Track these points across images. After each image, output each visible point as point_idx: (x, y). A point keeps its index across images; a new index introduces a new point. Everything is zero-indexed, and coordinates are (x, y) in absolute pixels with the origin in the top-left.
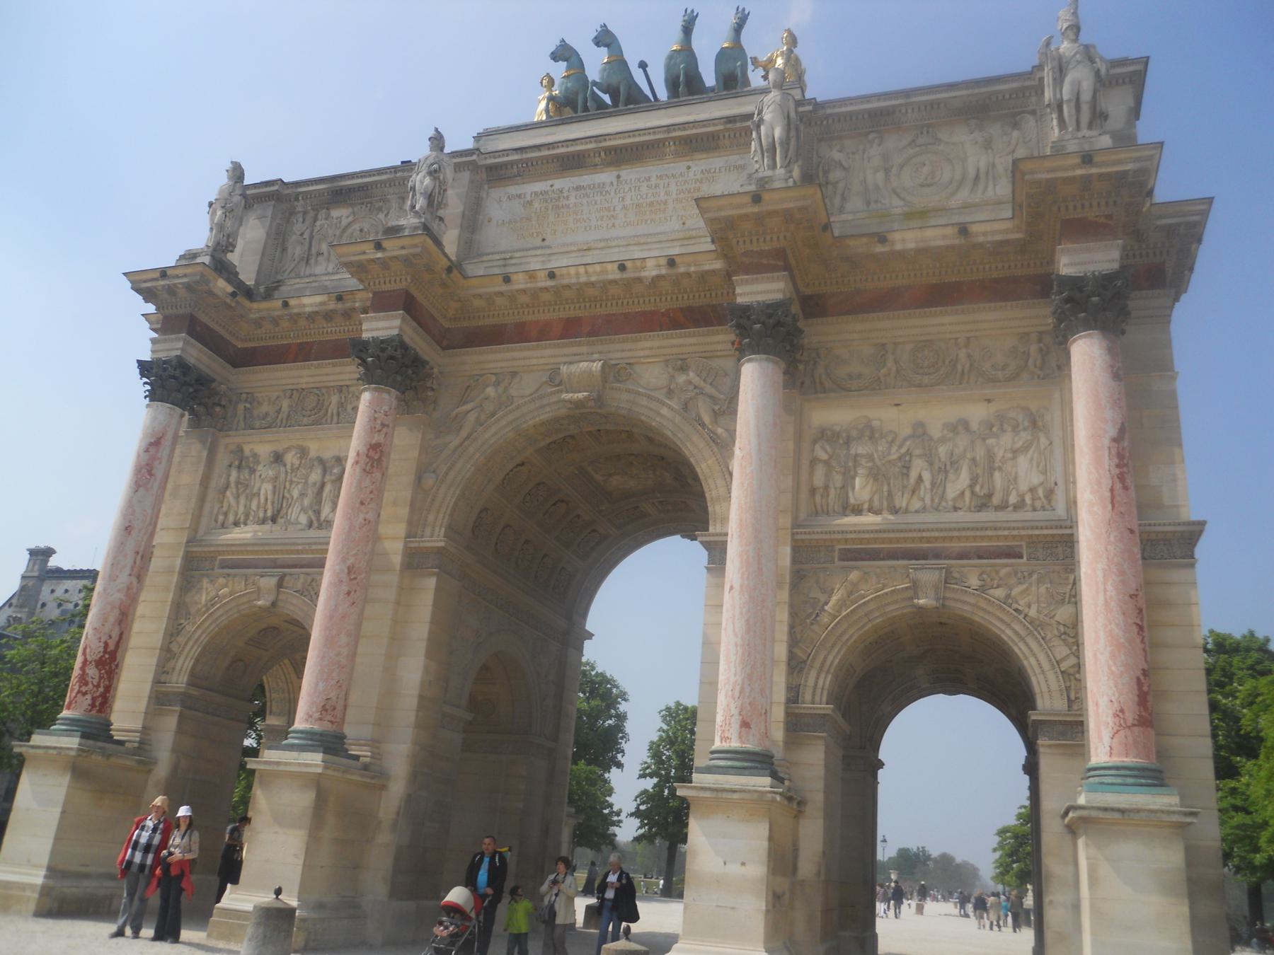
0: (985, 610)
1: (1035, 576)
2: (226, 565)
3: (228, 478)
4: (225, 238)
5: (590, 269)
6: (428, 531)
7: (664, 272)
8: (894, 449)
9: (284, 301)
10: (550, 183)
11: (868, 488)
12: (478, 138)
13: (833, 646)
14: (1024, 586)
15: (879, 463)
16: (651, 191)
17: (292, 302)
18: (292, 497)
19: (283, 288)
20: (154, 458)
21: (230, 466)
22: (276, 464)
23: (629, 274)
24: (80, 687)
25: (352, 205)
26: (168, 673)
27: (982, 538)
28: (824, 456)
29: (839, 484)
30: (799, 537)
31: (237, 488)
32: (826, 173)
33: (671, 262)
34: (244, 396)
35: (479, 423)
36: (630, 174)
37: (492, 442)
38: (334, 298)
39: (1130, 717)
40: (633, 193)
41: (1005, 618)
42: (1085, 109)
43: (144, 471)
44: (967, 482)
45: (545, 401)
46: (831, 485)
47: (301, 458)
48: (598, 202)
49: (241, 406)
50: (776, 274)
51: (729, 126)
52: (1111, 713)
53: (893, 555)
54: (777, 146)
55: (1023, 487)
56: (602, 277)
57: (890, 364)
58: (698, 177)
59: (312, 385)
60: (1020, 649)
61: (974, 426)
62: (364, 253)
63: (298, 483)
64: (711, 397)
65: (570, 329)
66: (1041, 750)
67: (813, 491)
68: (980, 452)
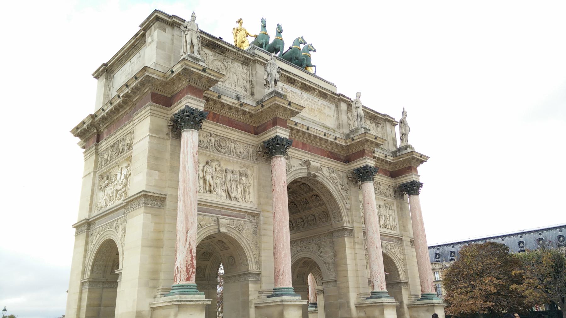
0: (391, 254)
5: (318, 132)
9: (219, 95)
17: (223, 97)
18: (218, 183)
23: (325, 138)
24: (193, 270)
25: (214, 51)
33: (335, 139)
38: (240, 104)
47: (219, 167)
51: (332, 94)
55: (392, 225)
56: (319, 135)
60: (397, 264)
62: (284, 104)
63: (219, 177)
65: (304, 147)
66: (402, 289)
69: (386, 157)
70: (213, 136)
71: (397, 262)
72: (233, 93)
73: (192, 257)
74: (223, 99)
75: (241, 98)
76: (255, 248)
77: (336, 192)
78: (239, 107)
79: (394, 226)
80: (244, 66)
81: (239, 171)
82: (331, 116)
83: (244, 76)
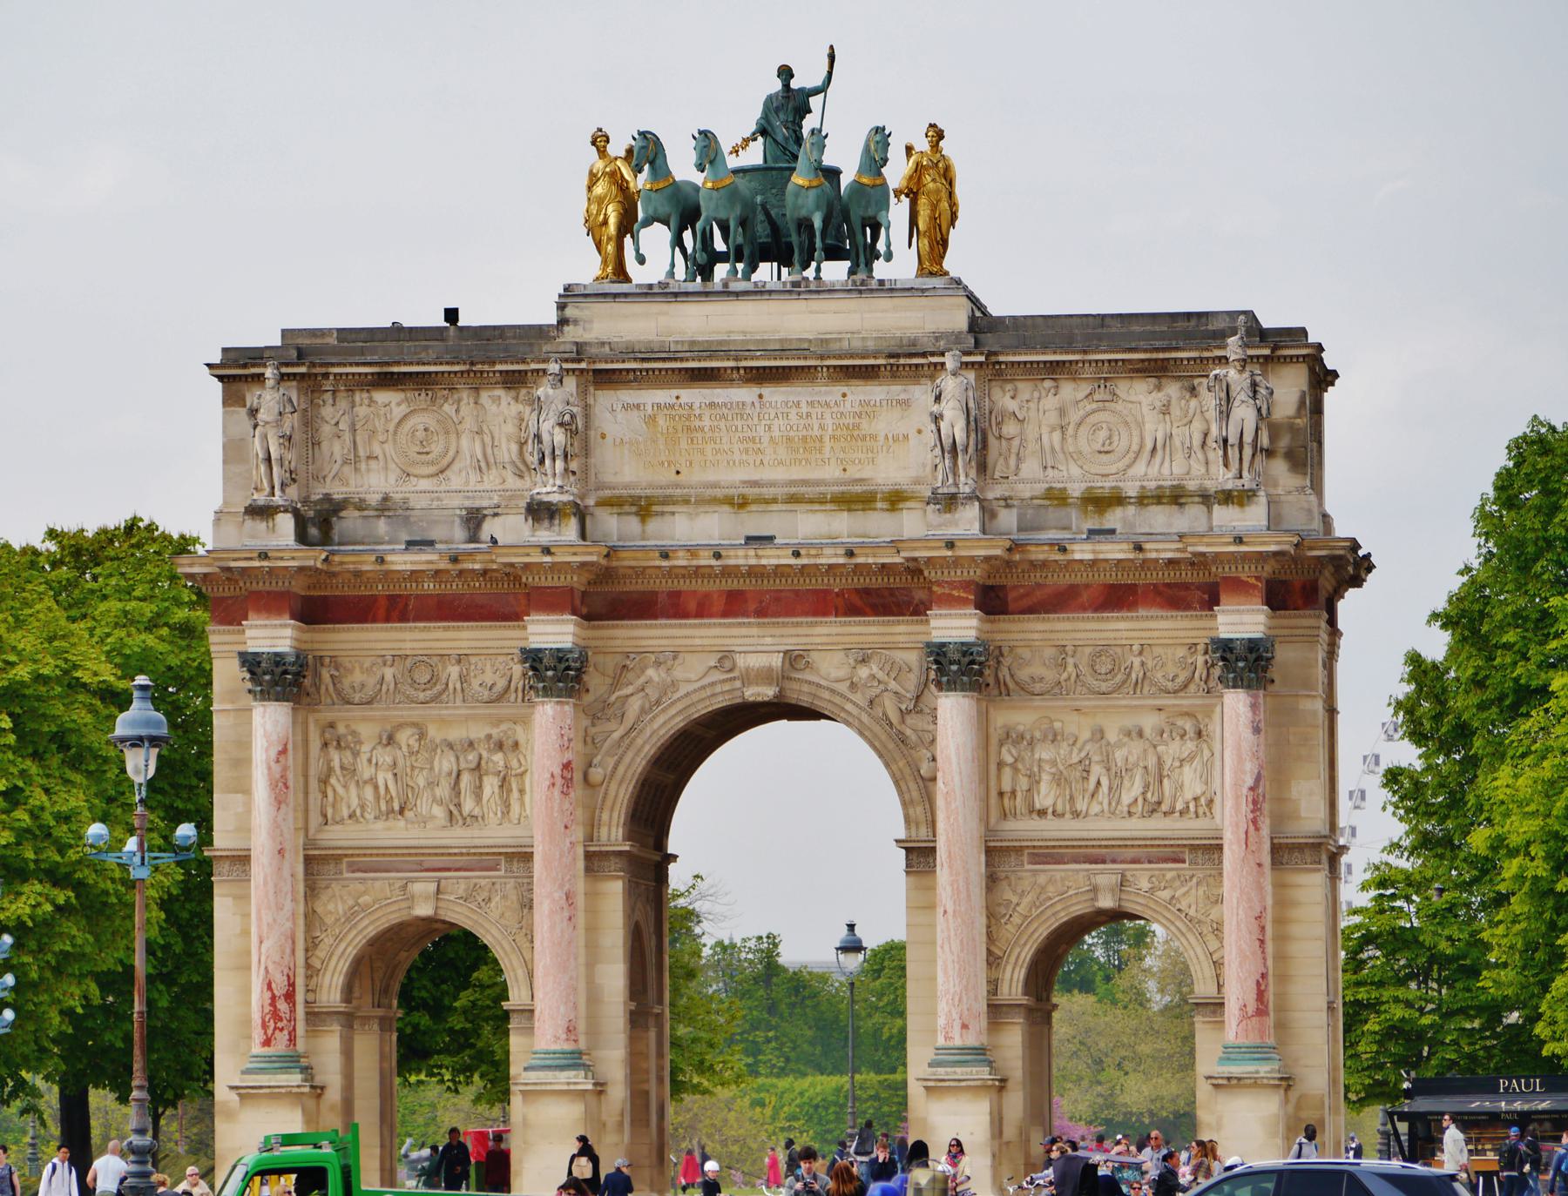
1: (1195, 880)
2: (354, 868)
3: (329, 764)
4: (288, 475)
5: (760, 552)
6: (604, 831)
7: (841, 560)
8: (1074, 755)
10: (675, 392)
11: (1053, 792)
12: (561, 307)
13: (1025, 944)
14: (1185, 889)
15: (1062, 768)
16: (802, 422)
17: (389, 558)
19: (343, 514)
20: (285, 769)
21: (325, 745)
22: (389, 748)
25: (403, 390)
26: (314, 991)
27: (1152, 846)
28: (1010, 760)
29: (1025, 787)
30: (992, 844)
31: (344, 776)
32: (998, 424)
34: (327, 660)
35: (643, 711)
36: (775, 394)
37: (662, 732)
39: (1251, 1009)
40: (781, 422)
41: (1168, 915)
42: (1248, 451)
43: (280, 784)
44: (1141, 790)
45: (718, 689)
46: (1018, 789)
47: (420, 739)
48: (740, 429)
49: (325, 675)
50: (968, 611)
51: (892, 361)
52: (1237, 1007)
53: (1076, 861)
54: (959, 448)
55: (1189, 795)
57: (1070, 668)
58: (857, 409)
59: (421, 652)
61: (1148, 732)
62: (528, 555)
63: (422, 769)
64: (896, 693)
66: (1197, 1025)
67: (1001, 794)
68: (1151, 761)
69: (1138, 548)
70: (389, 663)
71: (1183, 934)
72: (458, 512)
73: (273, 998)
74: (392, 563)
75: (485, 516)
76: (528, 944)
77: (877, 729)
78: (450, 566)
79: (1203, 801)
80: (513, 393)
81: (489, 737)
82: (906, 437)
83: (510, 428)
